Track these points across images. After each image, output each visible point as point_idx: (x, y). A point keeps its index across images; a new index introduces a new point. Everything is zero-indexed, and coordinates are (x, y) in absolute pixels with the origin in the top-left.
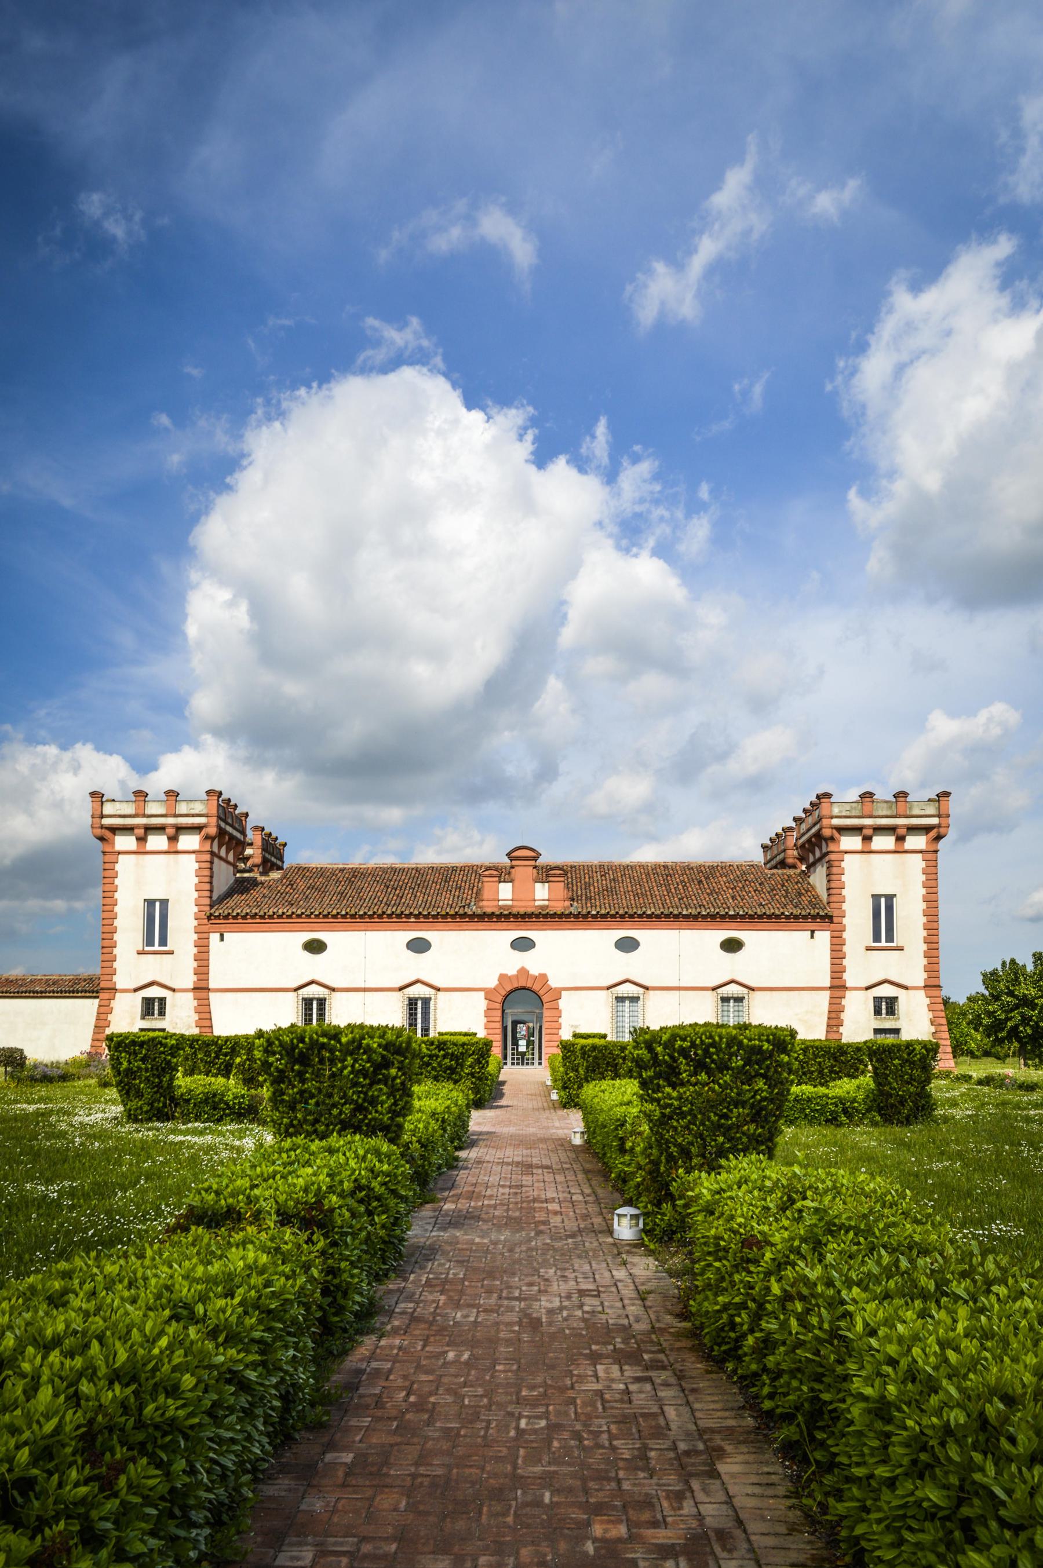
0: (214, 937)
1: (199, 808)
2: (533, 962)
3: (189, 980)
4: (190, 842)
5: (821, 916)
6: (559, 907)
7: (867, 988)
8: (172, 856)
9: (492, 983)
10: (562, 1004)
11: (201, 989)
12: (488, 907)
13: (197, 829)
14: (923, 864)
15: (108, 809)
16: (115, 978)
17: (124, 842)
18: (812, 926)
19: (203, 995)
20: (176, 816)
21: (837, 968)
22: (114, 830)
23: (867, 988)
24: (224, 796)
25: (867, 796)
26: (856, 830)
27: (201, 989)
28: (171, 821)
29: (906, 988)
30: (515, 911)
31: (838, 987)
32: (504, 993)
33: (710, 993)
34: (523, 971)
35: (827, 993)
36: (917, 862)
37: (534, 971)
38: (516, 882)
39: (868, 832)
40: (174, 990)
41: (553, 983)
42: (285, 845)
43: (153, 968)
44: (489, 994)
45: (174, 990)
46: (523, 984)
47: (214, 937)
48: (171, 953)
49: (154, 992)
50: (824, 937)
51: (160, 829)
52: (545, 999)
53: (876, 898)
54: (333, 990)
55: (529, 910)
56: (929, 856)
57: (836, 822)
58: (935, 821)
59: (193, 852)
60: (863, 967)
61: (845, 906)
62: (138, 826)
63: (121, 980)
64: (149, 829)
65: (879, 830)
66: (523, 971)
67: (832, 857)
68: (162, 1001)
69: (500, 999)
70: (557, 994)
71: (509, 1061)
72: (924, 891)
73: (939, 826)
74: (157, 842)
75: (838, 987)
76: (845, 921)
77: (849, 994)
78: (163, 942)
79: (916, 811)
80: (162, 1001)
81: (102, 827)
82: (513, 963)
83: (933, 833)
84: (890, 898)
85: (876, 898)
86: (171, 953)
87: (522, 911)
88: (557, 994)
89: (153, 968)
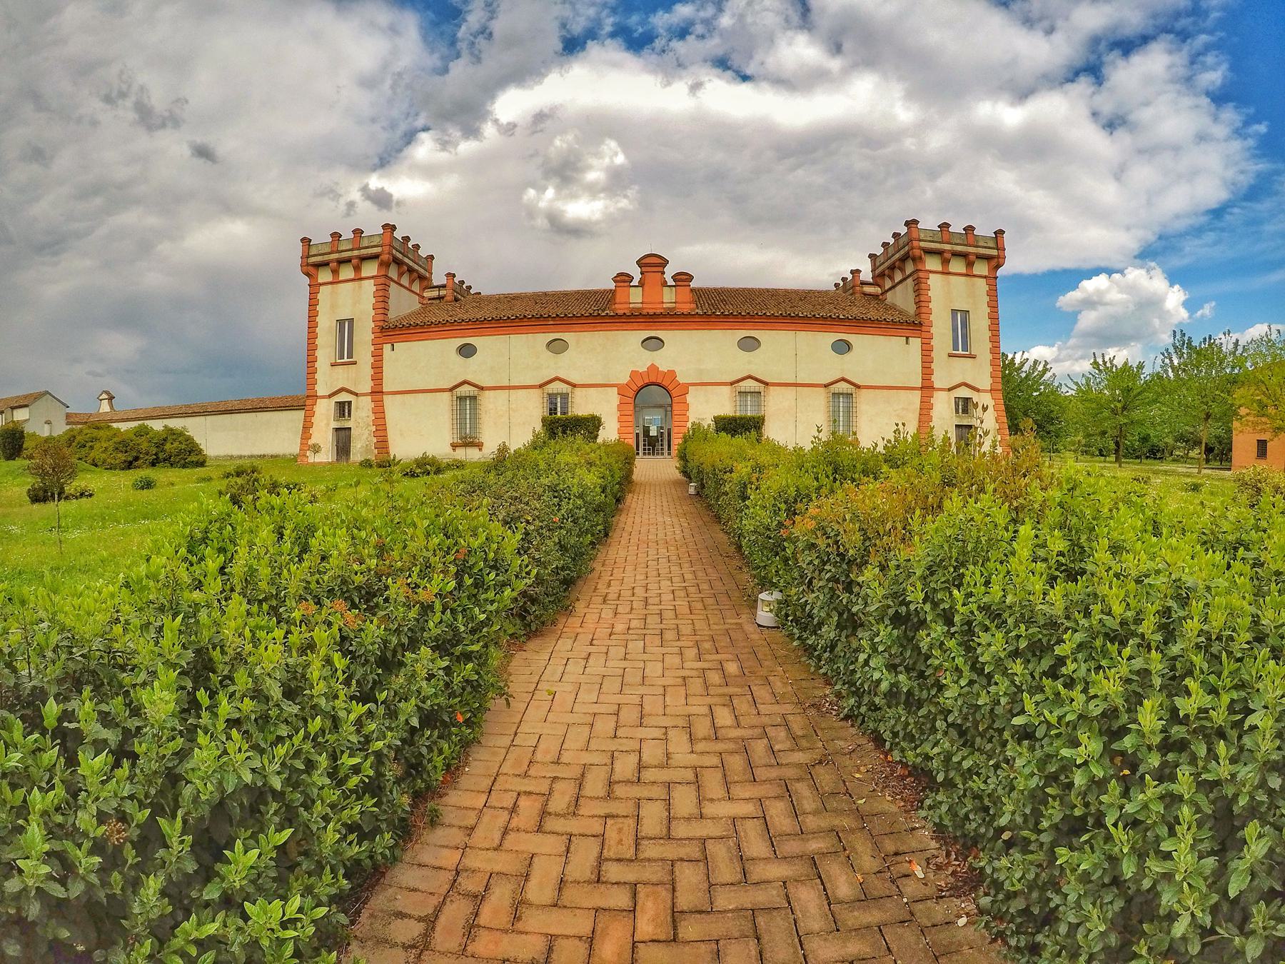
0: (387, 347)
1: (376, 241)
2: (664, 360)
3: (367, 386)
4: (370, 269)
5: (914, 325)
6: (686, 308)
7: (949, 390)
8: (356, 283)
9: (624, 379)
10: (689, 398)
11: (377, 393)
12: (620, 309)
13: (375, 257)
14: (987, 288)
15: (313, 251)
16: (317, 387)
17: (324, 276)
18: (908, 333)
19: (378, 397)
20: (359, 249)
21: (927, 371)
22: (318, 266)
23: (949, 390)
24: (398, 235)
25: (945, 226)
26: (939, 253)
27: (377, 393)
28: (356, 253)
29: (978, 390)
30: (644, 312)
31: (927, 388)
32: (635, 388)
33: (822, 390)
34: (653, 368)
35: (919, 393)
36: (982, 285)
37: (663, 368)
38: (646, 287)
39: (947, 255)
40: (356, 395)
41: (681, 379)
42: (432, 257)
43: (342, 377)
44: (622, 390)
45: (356, 395)
46: (653, 379)
47: (387, 347)
48: (355, 363)
49: (344, 397)
50: (916, 343)
51: (348, 261)
52: (674, 393)
53: (954, 312)
54: (482, 388)
55: (658, 312)
56: (992, 281)
57: (922, 244)
58: (994, 252)
59: (372, 277)
60: (947, 372)
61: (932, 318)
62: (332, 261)
63: (321, 390)
64: (341, 262)
65: (956, 254)
66: (653, 368)
67: (921, 274)
68: (350, 403)
69: (632, 394)
70: (685, 388)
71: (641, 452)
72: (988, 310)
73: (998, 257)
74: (347, 272)
75: (927, 388)
76: (933, 330)
77: (936, 394)
78: (350, 356)
79: (981, 244)
80: (350, 403)
81: (308, 265)
82: (642, 360)
83: (994, 263)
84: (966, 313)
85: (954, 312)
86: (355, 363)
87: (651, 312)
88: (685, 388)
89: (342, 377)
